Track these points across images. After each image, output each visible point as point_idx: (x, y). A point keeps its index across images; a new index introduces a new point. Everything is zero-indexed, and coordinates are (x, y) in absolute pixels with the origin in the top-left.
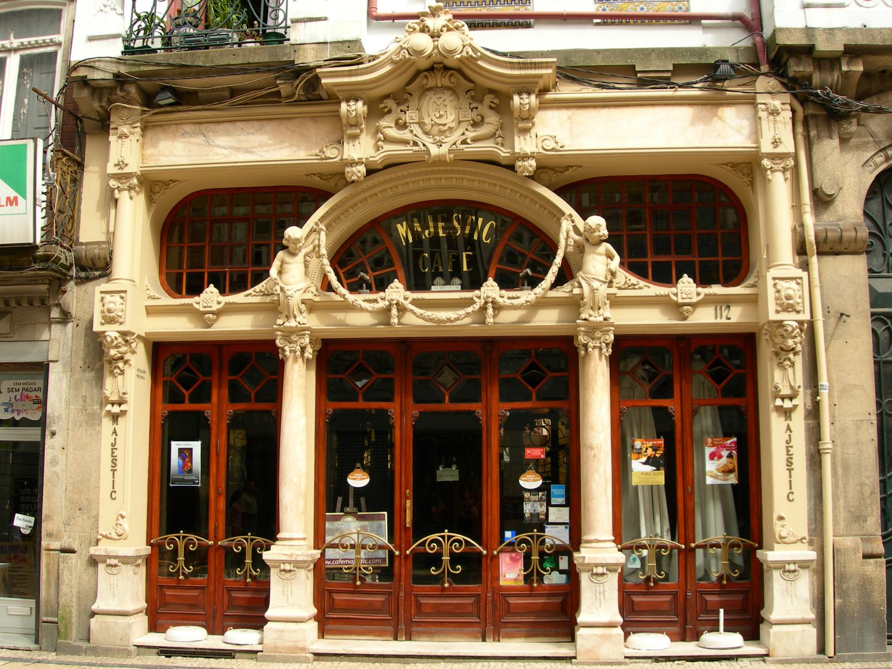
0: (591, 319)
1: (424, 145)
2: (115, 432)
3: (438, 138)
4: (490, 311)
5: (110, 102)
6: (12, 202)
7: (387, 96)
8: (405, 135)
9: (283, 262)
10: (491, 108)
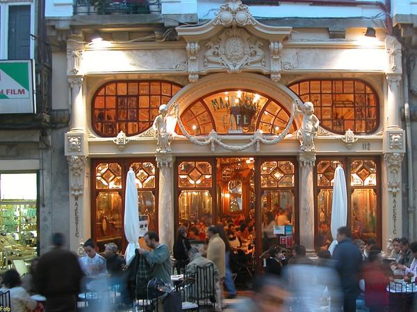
2: (76, 204)
4: (258, 145)
5: (67, 38)
6: (21, 92)
7: (209, 40)
8: (220, 61)
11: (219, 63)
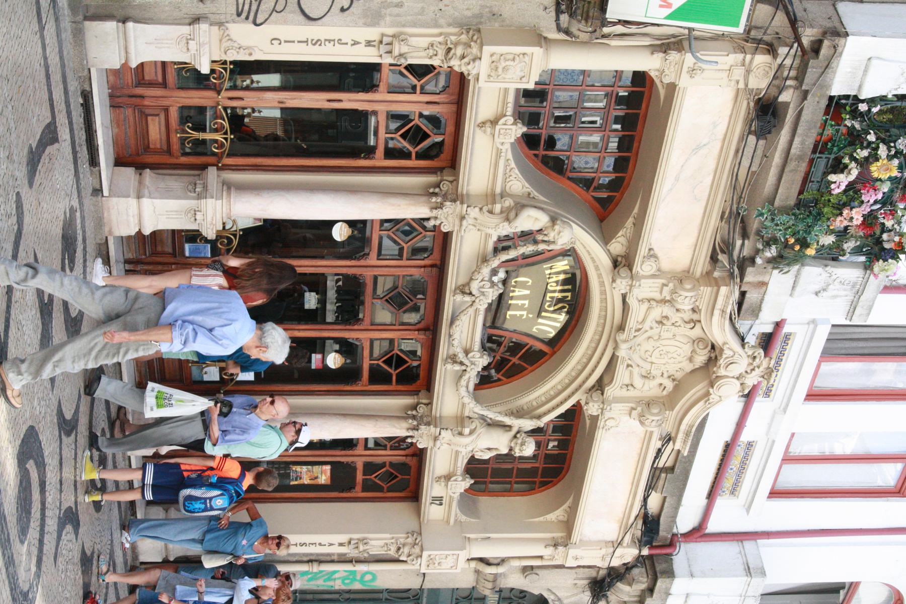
2: (356, 43)
10: (661, 384)
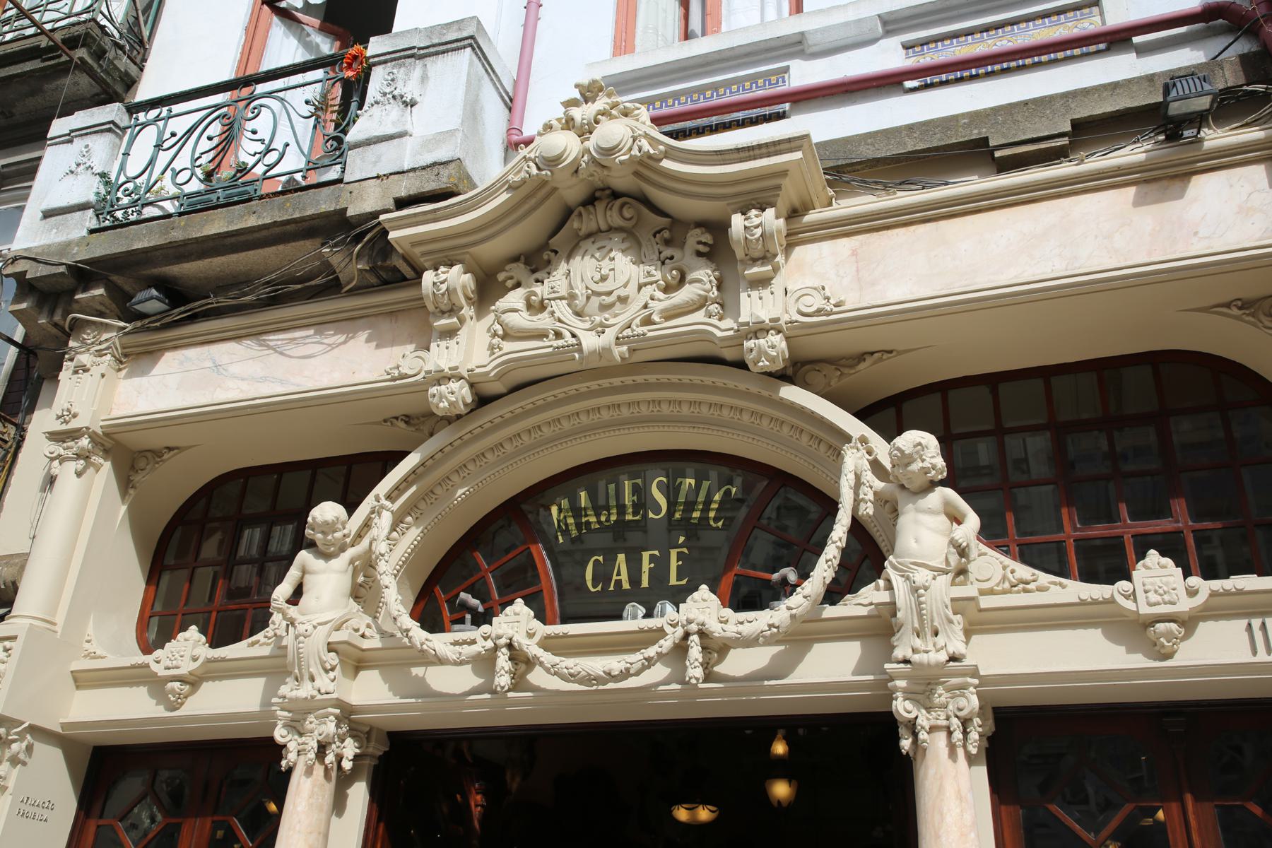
0: (916, 658)
1: (574, 336)
3: (598, 319)
4: (695, 652)
7: (516, 259)
8: (543, 321)
9: (304, 572)
11: (541, 335)
